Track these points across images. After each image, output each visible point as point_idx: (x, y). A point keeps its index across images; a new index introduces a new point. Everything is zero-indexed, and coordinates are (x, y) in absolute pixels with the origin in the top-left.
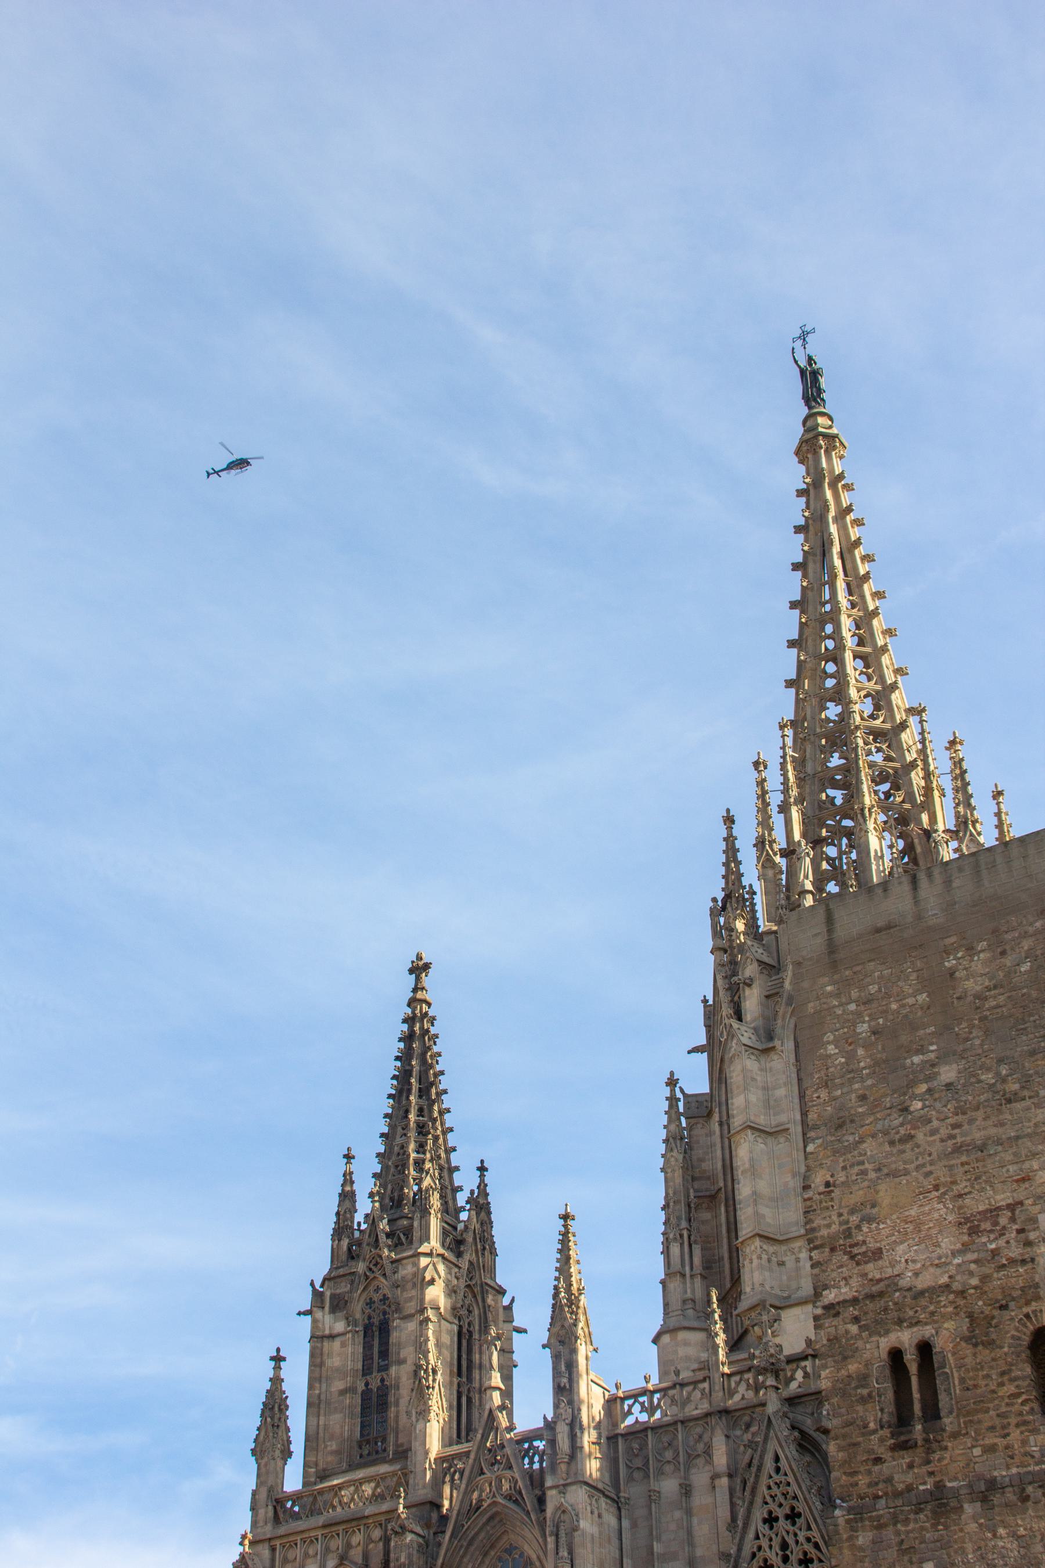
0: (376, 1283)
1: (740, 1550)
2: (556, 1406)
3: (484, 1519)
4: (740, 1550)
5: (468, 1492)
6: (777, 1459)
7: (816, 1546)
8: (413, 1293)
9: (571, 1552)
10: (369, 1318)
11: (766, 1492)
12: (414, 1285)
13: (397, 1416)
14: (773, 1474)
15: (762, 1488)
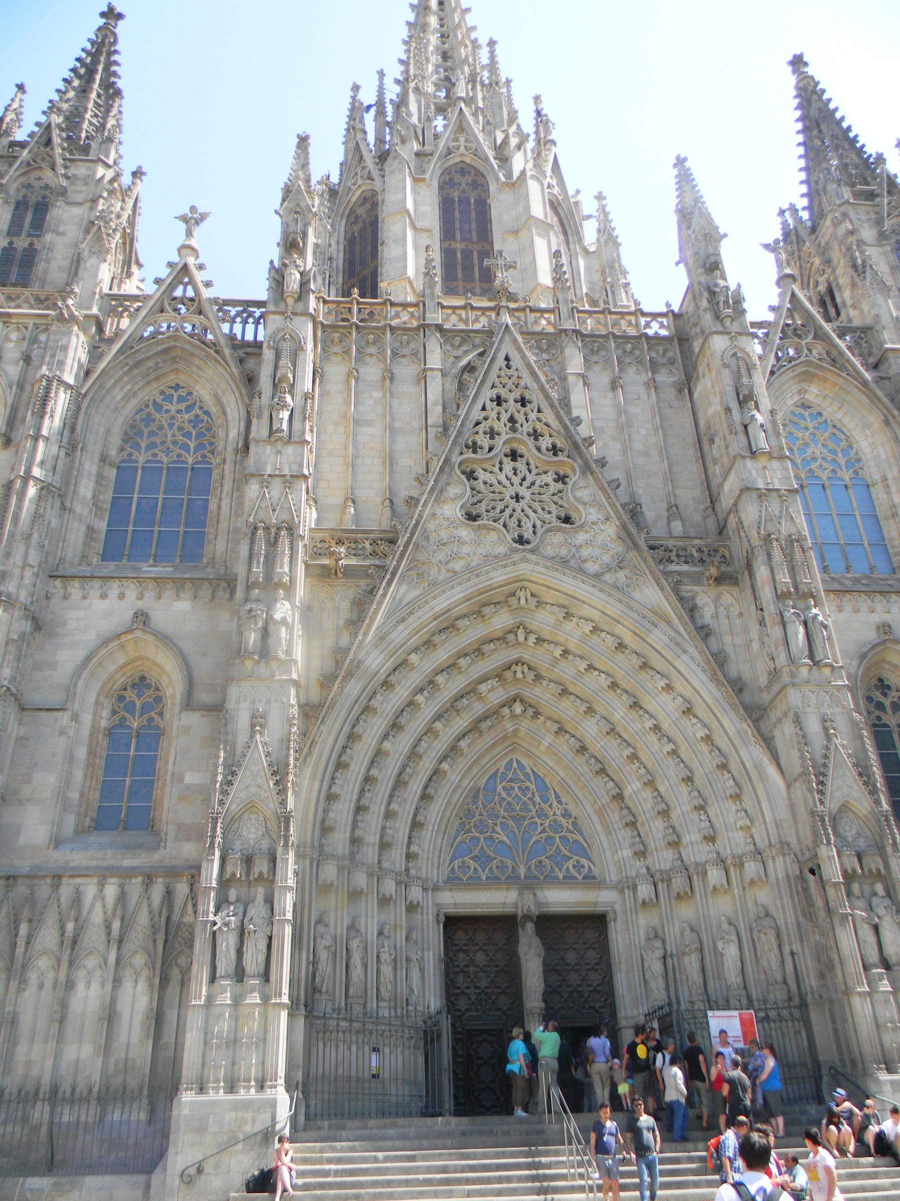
0: (39, 173)
1: (468, 414)
2: (282, 258)
3: (160, 348)
4: (468, 414)
5: (145, 323)
6: (507, 359)
7: (547, 425)
8: (84, 188)
9: (294, 366)
10: (25, 197)
11: (497, 381)
12: (86, 184)
13: (45, 272)
14: (504, 367)
15: (493, 377)
